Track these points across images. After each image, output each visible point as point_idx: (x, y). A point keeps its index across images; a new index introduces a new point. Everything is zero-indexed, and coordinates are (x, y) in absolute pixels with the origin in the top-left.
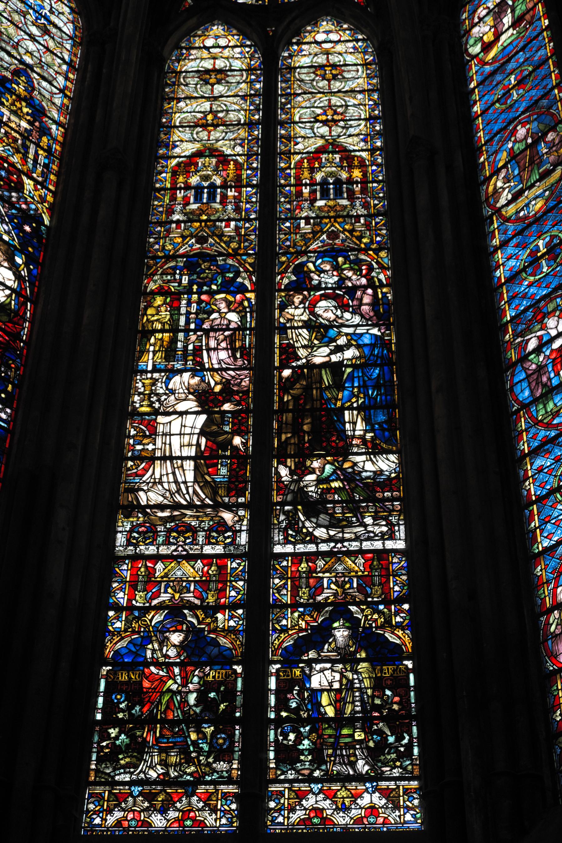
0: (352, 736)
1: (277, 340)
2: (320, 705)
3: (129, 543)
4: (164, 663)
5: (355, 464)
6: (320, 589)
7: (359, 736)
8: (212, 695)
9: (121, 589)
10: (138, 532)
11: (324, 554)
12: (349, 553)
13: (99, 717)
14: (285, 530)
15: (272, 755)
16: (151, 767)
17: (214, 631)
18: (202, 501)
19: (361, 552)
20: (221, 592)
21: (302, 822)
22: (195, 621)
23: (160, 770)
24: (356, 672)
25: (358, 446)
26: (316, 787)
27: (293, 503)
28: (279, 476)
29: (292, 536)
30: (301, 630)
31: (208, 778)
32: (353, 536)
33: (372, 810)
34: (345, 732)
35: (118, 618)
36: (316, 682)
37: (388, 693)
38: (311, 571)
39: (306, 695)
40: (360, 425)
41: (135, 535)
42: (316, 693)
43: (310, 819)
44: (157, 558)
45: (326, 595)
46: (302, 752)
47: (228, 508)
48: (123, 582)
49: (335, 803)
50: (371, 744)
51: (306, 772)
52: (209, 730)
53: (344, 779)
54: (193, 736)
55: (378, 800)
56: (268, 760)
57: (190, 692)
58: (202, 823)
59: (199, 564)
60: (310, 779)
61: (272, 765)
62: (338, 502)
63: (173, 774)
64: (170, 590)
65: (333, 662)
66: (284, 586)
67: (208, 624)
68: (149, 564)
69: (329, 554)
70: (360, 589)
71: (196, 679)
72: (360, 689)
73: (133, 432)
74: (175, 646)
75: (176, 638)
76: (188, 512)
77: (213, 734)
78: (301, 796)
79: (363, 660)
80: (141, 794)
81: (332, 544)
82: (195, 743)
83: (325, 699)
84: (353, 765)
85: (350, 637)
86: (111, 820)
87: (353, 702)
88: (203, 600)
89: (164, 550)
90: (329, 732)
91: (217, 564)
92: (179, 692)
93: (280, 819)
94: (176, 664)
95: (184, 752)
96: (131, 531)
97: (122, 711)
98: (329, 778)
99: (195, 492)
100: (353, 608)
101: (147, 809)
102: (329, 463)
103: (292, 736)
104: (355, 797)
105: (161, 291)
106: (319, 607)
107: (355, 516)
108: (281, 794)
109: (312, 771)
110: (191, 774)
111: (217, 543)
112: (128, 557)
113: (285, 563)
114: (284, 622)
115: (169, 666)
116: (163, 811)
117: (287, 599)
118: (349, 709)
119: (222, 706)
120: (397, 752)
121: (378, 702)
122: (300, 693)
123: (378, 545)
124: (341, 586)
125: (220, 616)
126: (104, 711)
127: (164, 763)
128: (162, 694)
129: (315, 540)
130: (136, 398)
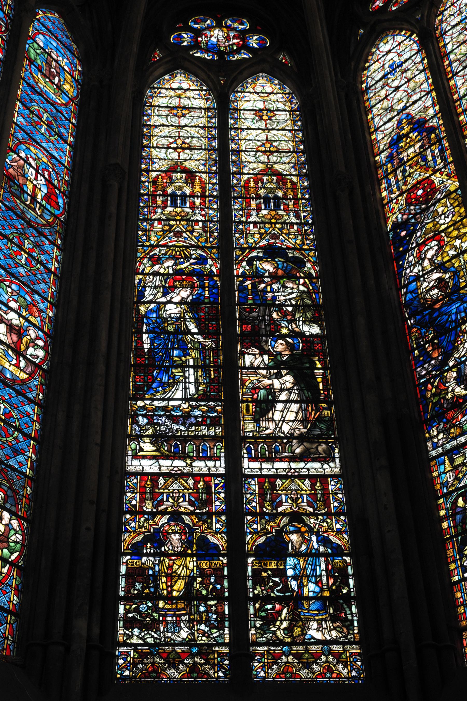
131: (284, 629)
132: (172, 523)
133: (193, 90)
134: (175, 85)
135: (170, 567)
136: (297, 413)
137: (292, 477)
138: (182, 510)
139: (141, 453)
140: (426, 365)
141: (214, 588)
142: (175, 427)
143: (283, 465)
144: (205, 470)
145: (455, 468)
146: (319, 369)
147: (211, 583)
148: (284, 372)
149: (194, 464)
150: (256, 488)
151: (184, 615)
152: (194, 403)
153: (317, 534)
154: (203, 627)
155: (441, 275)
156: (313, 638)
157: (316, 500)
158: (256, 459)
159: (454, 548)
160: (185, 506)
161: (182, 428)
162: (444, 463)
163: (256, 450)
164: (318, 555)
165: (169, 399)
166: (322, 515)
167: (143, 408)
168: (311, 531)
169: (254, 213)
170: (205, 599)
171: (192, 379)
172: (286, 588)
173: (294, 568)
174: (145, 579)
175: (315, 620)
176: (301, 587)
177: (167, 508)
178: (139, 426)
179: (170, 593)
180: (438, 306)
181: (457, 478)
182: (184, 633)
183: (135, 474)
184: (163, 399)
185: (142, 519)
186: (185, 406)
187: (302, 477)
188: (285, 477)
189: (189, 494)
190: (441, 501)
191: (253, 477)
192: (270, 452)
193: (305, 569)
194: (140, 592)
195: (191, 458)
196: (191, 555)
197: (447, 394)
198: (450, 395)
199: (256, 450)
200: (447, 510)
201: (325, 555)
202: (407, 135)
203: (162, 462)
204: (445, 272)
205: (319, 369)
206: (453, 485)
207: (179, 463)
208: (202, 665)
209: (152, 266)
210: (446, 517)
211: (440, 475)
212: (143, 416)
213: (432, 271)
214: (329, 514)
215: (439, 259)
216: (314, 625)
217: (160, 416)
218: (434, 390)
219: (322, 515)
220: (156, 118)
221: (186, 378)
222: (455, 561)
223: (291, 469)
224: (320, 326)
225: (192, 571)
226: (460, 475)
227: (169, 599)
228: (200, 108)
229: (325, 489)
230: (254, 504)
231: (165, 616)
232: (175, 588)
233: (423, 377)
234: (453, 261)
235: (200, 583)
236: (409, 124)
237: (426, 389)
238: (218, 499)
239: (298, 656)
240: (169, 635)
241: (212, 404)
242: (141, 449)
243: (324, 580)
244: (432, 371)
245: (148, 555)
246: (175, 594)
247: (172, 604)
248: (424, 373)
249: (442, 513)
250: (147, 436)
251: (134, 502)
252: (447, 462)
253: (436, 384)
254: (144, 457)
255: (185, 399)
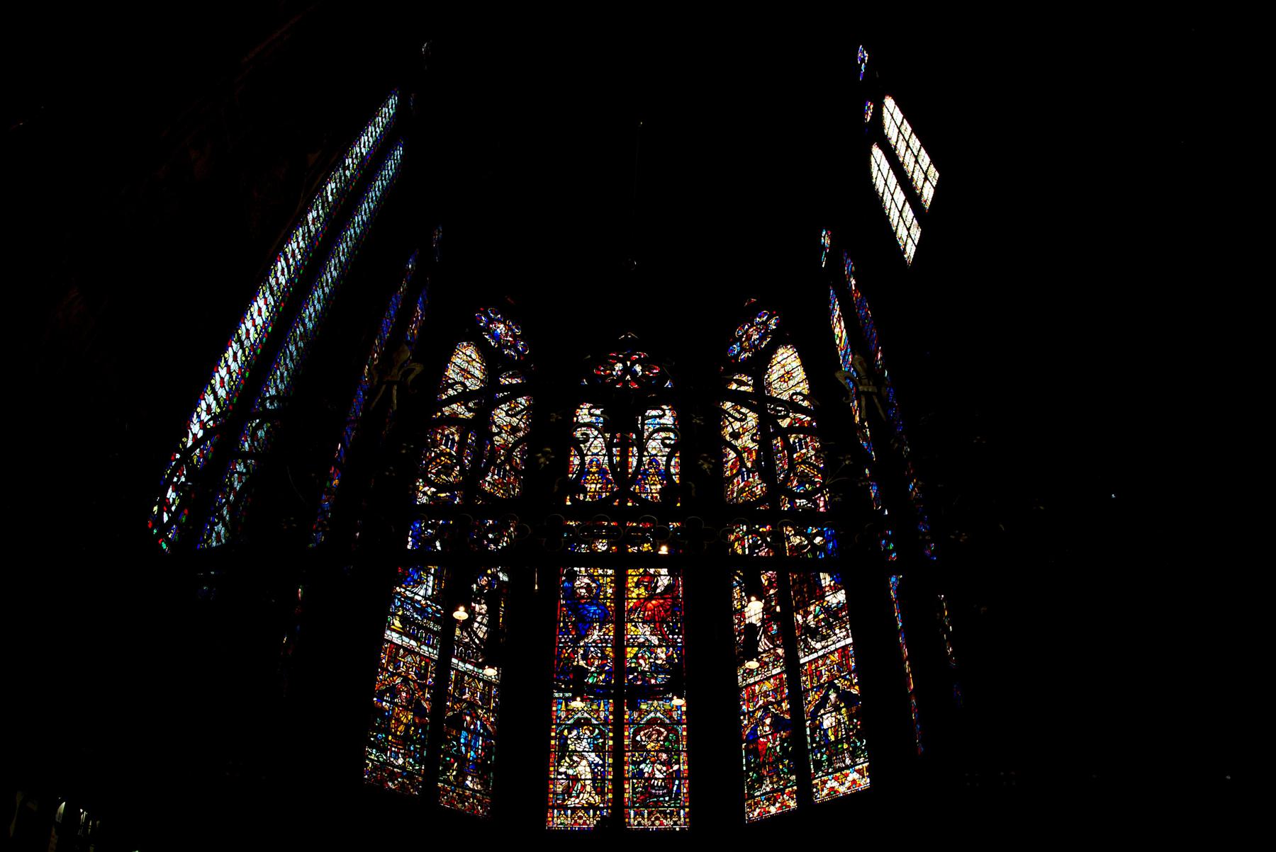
0: (842, 747)
1: (787, 546)
2: (828, 736)
3: (743, 680)
4: (765, 735)
5: (828, 602)
6: (820, 676)
7: (845, 746)
8: (785, 745)
9: (744, 704)
10: (746, 673)
11: (819, 657)
12: (832, 653)
13: (744, 768)
14: (803, 650)
15: (812, 766)
16: (767, 786)
17: (782, 712)
18: (768, 647)
19: (836, 650)
20: (782, 692)
21: (827, 795)
22: (774, 710)
23: (771, 786)
24: (841, 714)
25: (828, 591)
26: (830, 777)
27: (805, 634)
28: (797, 620)
29: (807, 652)
30: (816, 700)
31: (789, 785)
32: (832, 642)
33: (854, 782)
34: (840, 746)
35: (745, 719)
36: (825, 726)
37: (855, 721)
38: (817, 667)
39: (822, 732)
40: (828, 579)
41: (745, 675)
42: (826, 731)
43: (830, 793)
44: (755, 683)
45: (825, 677)
46: (823, 762)
47: (779, 646)
48: (744, 700)
49: (839, 782)
50: (851, 749)
51: (826, 771)
52: (786, 762)
53: (841, 769)
54: (781, 767)
55: (855, 776)
56: (811, 770)
57: (777, 746)
58: (789, 806)
59: (772, 680)
60: (828, 774)
61: (813, 771)
62: (824, 626)
63: (775, 786)
64: (762, 698)
65: (831, 712)
66: (807, 680)
67: (779, 710)
68: (753, 688)
69: (824, 656)
70: (838, 670)
71: (778, 739)
72: (844, 723)
73: (737, 621)
74: (768, 725)
75: (768, 721)
76: (764, 655)
77: (788, 763)
78: (824, 783)
79: (843, 707)
80: (765, 799)
81: (824, 650)
82: (782, 770)
83: (830, 733)
84: (844, 762)
85: (837, 697)
86: (756, 814)
87: (841, 731)
88: (775, 698)
89: (757, 679)
90: (833, 748)
91: (779, 678)
92: (773, 747)
93: (818, 796)
94: (769, 734)
95: (778, 775)
96: (744, 673)
97: (753, 763)
98: (836, 771)
99: (766, 644)
100: (836, 681)
101: (768, 806)
102: (818, 605)
103: (819, 755)
104: (846, 776)
105: (737, 539)
106: (820, 686)
107: (831, 631)
108: (817, 784)
109: (828, 770)
110: (782, 785)
111: (777, 667)
112: (745, 687)
113: (806, 668)
114: (809, 699)
115: (767, 736)
116: (774, 805)
117: (809, 687)
118: (840, 735)
119: (790, 749)
120: (861, 749)
121: (851, 727)
122: (820, 733)
123: (842, 643)
124: (829, 671)
125: (783, 704)
126: (746, 765)
127: (772, 783)
128: (767, 750)
129: (816, 651)
130: (735, 602)
131: (454, 776)
132: (403, 684)
133: (478, 362)
134: (468, 353)
135: (398, 714)
136: (485, 634)
137: (474, 678)
138: (410, 677)
139: (393, 627)
140: (566, 636)
141: (421, 736)
142: (416, 616)
143: (471, 667)
144: (427, 654)
145: (567, 711)
146: (502, 607)
147: (419, 733)
148: (483, 601)
149: (422, 647)
150: (453, 677)
151: (402, 749)
152: (429, 603)
153: (481, 720)
154: (411, 760)
155: (589, 582)
156: (467, 786)
157: (484, 698)
158: (456, 657)
159: (555, 758)
160: (412, 675)
161: (419, 618)
162: (561, 704)
163: (458, 650)
164: (479, 734)
165: (416, 594)
166: (485, 709)
167: (399, 593)
168: (478, 718)
169: (490, 474)
170: (414, 743)
171: (431, 584)
172: (459, 750)
173: (465, 739)
174: (383, 717)
175: (470, 775)
176: (467, 752)
177: (401, 672)
178: (395, 606)
179: (396, 731)
180: (583, 601)
181: (567, 717)
182: (401, 761)
183: (388, 641)
184: (412, 592)
185: (387, 675)
186: (423, 602)
187: (480, 680)
188: (470, 676)
189: (416, 667)
190: (554, 727)
191: (453, 669)
192: (465, 656)
193: (471, 741)
194: (380, 725)
195: (421, 641)
196: (411, 711)
197: (574, 661)
198: (575, 663)
199: (458, 651)
200: (556, 734)
201: (482, 735)
202: (594, 474)
203: (404, 638)
204: (594, 581)
205: (502, 607)
206: (564, 720)
207: (413, 643)
208: (408, 784)
209: (424, 486)
210: (554, 738)
211: (557, 710)
212: (399, 600)
213: (585, 576)
214: (488, 710)
215: (592, 571)
216: (470, 778)
217: (407, 603)
218: (566, 655)
219: (485, 709)
220: (451, 372)
221: (428, 582)
222: (554, 766)
223: (474, 671)
224: (508, 576)
225: (410, 721)
226: (570, 716)
227: (394, 735)
228: (478, 378)
229: (490, 692)
230: (450, 688)
231: (392, 746)
232: (399, 729)
233: (562, 643)
234: (600, 578)
235: (413, 731)
236: (597, 467)
237: (561, 652)
238: (431, 677)
239: (458, 794)
240: (392, 759)
241: (439, 607)
242: (393, 624)
243: (480, 751)
244: (568, 642)
245: (387, 701)
246: (398, 733)
247: (396, 739)
248: (563, 640)
249: (553, 734)
250: (398, 615)
251: (384, 661)
252: (564, 704)
253: (569, 651)
254: (394, 630)
255: (425, 597)
